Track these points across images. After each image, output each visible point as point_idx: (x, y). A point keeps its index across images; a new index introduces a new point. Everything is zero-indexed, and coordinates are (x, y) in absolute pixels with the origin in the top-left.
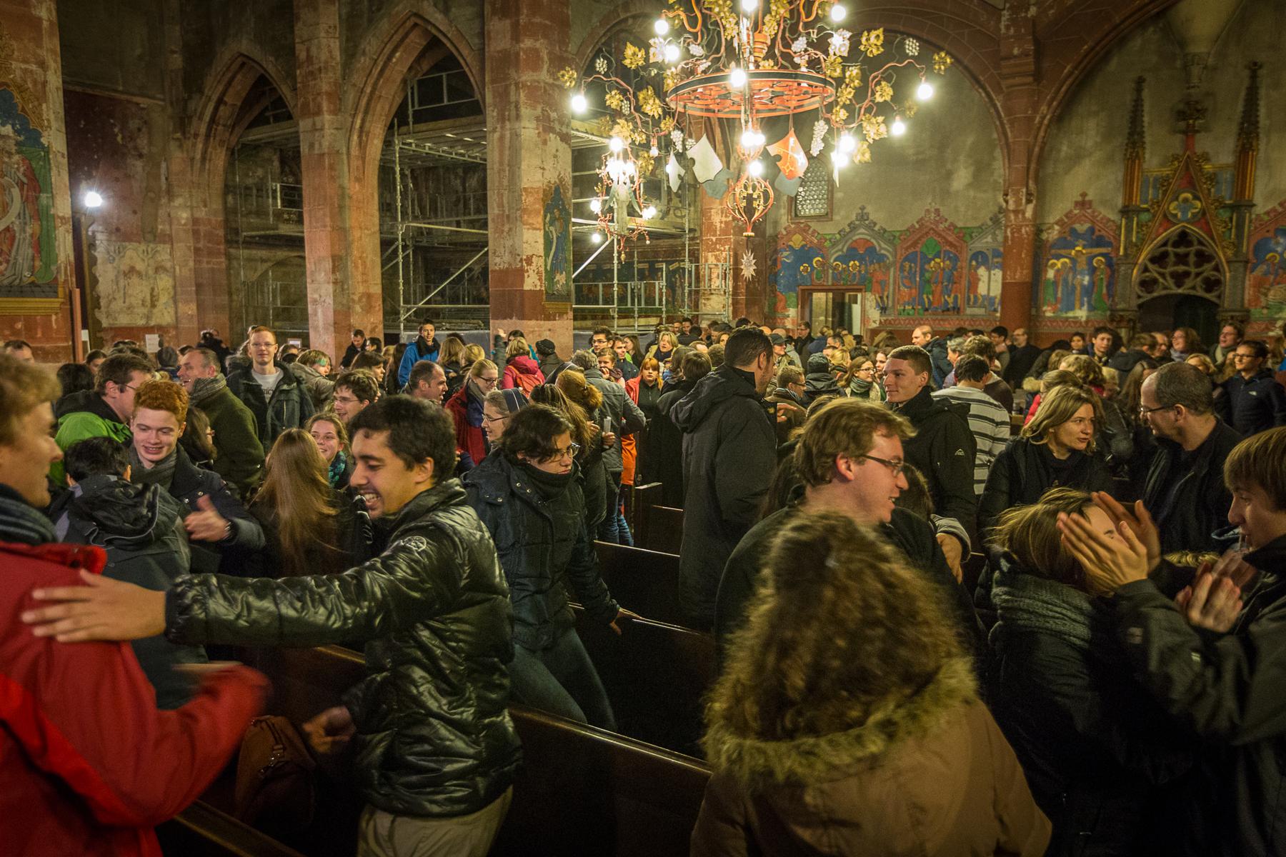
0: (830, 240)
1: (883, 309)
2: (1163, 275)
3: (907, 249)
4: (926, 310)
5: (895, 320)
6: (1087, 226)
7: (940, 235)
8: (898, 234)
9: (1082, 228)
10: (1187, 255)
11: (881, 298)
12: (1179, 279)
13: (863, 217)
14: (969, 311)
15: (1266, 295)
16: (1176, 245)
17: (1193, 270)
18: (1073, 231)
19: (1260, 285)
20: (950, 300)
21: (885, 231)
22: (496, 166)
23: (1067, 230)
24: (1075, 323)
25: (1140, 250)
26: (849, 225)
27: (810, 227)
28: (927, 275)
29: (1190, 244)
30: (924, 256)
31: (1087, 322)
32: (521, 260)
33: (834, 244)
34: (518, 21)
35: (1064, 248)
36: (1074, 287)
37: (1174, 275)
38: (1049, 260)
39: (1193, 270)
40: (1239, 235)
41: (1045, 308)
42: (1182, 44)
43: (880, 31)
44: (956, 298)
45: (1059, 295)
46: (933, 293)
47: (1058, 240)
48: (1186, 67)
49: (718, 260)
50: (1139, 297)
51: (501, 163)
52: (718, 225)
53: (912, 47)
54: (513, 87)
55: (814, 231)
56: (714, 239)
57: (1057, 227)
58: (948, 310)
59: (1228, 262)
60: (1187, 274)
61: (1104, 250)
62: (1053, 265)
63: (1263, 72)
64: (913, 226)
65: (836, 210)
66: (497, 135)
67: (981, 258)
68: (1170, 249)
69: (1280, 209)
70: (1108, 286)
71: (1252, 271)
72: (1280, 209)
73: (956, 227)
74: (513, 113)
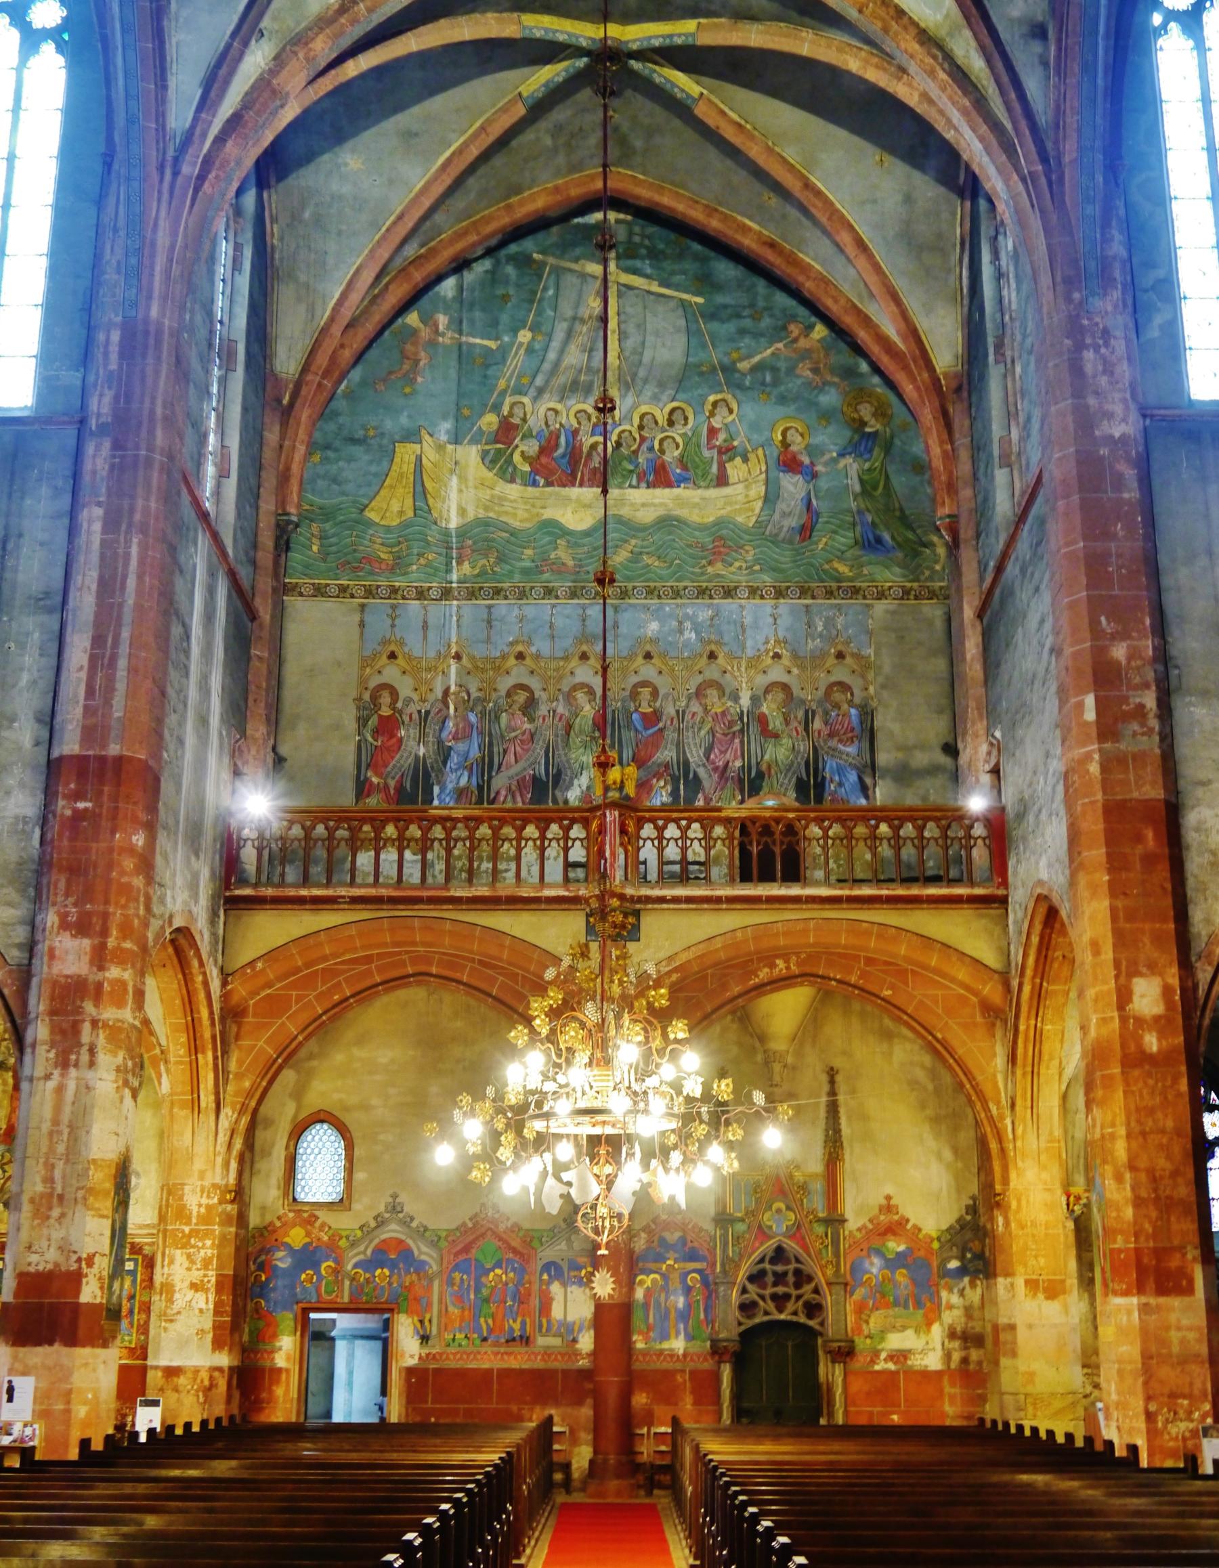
0: (347, 1237)
1: (425, 1339)
2: (763, 1298)
3: (457, 1254)
4: (485, 1339)
5: (441, 1354)
6: (677, 1235)
7: (501, 1239)
8: (444, 1234)
9: (673, 1237)
10: (785, 1274)
11: (421, 1322)
12: (780, 1301)
13: (395, 1208)
14: (541, 1341)
15: (867, 1322)
16: (773, 1261)
17: (794, 1293)
18: (662, 1241)
19: (860, 1309)
20: (517, 1326)
21: (426, 1229)
22: (46, 1126)
23: (656, 1238)
24: (672, 1356)
25: (738, 1267)
26: (376, 1218)
27: (317, 1218)
28: (485, 1292)
29: (788, 1262)
30: (479, 1263)
31: (685, 1355)
32: (79, 1260)
33: (353, 1244)
34: (103, 946)
35: (656, 1261)
36: (667, 1310)
37: (774, 1297)
38: (636, 1276)
39: (794, 1293)
40: (837, 1254)
41: (635, 1338)
42: (762, 1038)
43: (729, 1081)
44: (523, 1323)
45: (651, 1320)
46: (493, 1317)
47: (648, 1249)
48: (767, 1063)
49: (193, 1262)
50: (740, 1324)
51: (56, 1122)
52: (195, 1209)
53: (759, 1098)
54: (86, 1027)
55: (323, 1225)
56: (187, 1229)
57: (643, 1235)
58: (514, 1339)
59: (829, 1284)
60: (787, 1297)
61: (698, 1265)
62: (642, 1282)
63: (839, 1078)
64: (464, 1224)
65: (355, 1196)
66: (51, 1085)
67: (554, 1270)
68: (767, 1266)
69: (870, 1226)
70: (705, 1310)
71: (852, 1294)
72: (870, 1226)
73: (520, 1229)
74: (85, 1057)
